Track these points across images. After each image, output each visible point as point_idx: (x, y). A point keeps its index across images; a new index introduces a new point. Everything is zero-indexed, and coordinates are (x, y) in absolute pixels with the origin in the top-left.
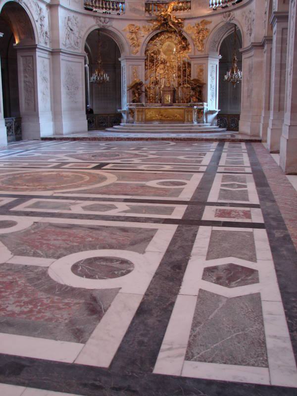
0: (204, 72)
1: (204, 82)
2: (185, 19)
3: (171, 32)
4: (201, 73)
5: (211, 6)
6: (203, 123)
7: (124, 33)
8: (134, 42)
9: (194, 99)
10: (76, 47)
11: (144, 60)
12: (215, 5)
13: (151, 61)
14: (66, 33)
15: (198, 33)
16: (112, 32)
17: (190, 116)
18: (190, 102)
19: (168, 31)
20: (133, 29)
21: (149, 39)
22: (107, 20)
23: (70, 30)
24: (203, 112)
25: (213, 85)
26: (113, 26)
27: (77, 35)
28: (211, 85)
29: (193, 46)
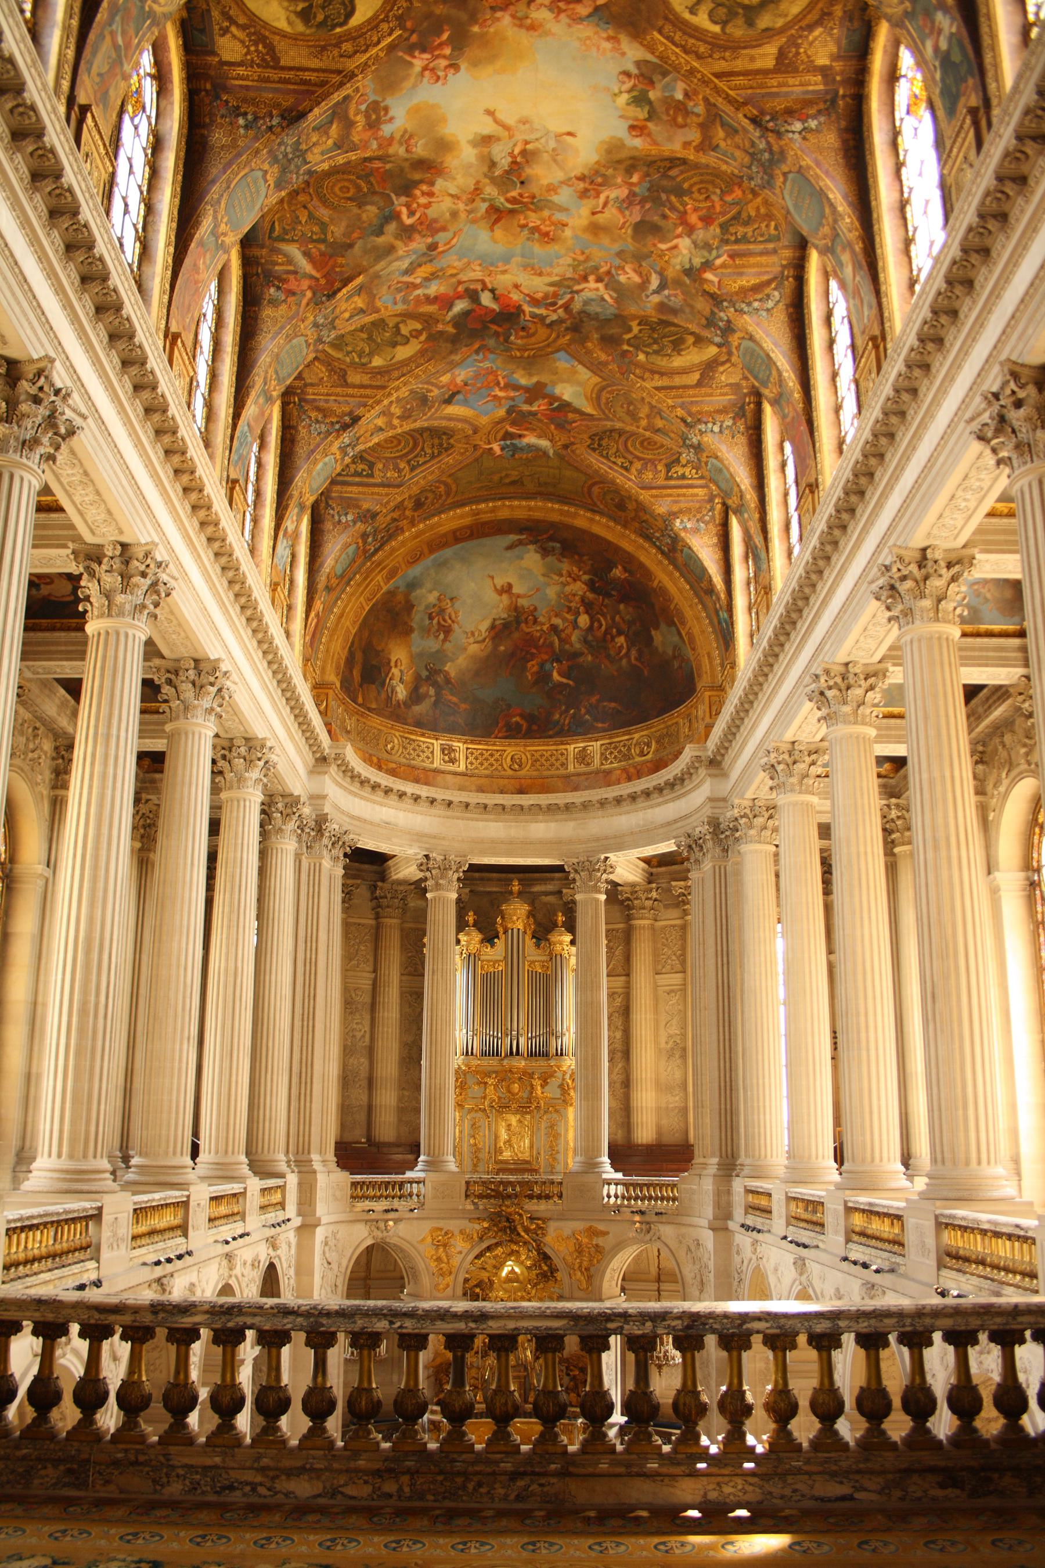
3: (516, 1243)
12: (612, 1200)
15: (579, 1250)
19: (511, 1241)
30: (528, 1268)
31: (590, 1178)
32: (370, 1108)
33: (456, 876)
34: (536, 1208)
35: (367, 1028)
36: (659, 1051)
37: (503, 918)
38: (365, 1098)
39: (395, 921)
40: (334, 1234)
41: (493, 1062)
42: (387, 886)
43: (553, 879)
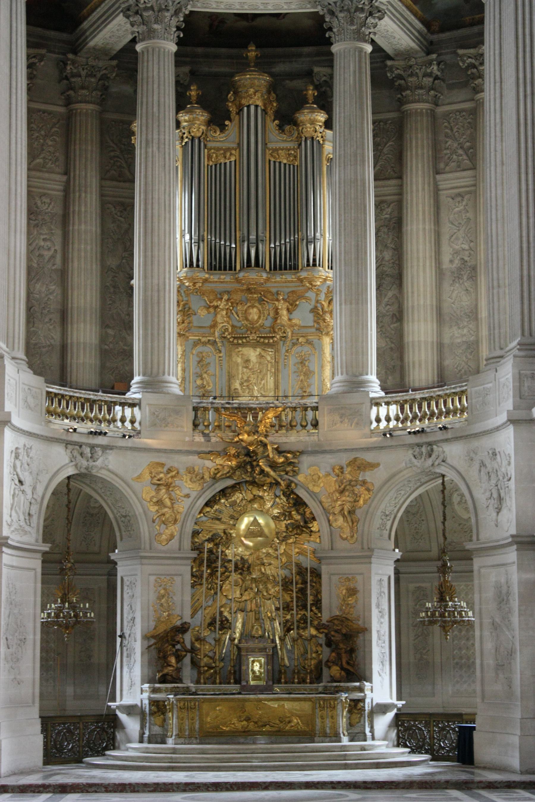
0: (360, 595)
1: (360, 623)
2: (302, 453)
3: (260, 486)
4: (351, 601)
5: (374, 424)
6: (365, 740)
7: (137, 486)
8: (166, 510)
9: (335, 670)
10: (27, 528)
11: (189, 562)
13: (209, 561)
14: (12, 493)
16: (103, 481)
17: (328, 723)
18: (318, 678)
19: (253, 483)
20: (162, 475)
21: (202, 502)
22: (99, 451)
23: (17, 482)
24: (363, 709)
25: (382, 632)
26: (110, 467)
27: (29, 496)
28: (378, 631)
29: (325, 524)
30: (275, 518)
31: (354, 398)
32: (64, 349)
33: (174, 22)
34: (284, 440)
35: (58, 247)
36: (440, 273)
37: (236, 93)
38: (57, 336)
39: (91, 107)
40: (28, 450)
41: (226, 277)
42: (81, 59)
43: (300, 55)
